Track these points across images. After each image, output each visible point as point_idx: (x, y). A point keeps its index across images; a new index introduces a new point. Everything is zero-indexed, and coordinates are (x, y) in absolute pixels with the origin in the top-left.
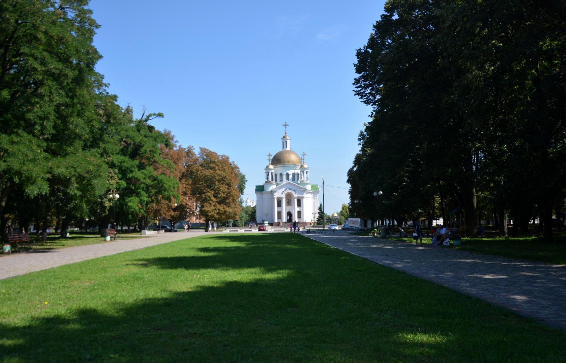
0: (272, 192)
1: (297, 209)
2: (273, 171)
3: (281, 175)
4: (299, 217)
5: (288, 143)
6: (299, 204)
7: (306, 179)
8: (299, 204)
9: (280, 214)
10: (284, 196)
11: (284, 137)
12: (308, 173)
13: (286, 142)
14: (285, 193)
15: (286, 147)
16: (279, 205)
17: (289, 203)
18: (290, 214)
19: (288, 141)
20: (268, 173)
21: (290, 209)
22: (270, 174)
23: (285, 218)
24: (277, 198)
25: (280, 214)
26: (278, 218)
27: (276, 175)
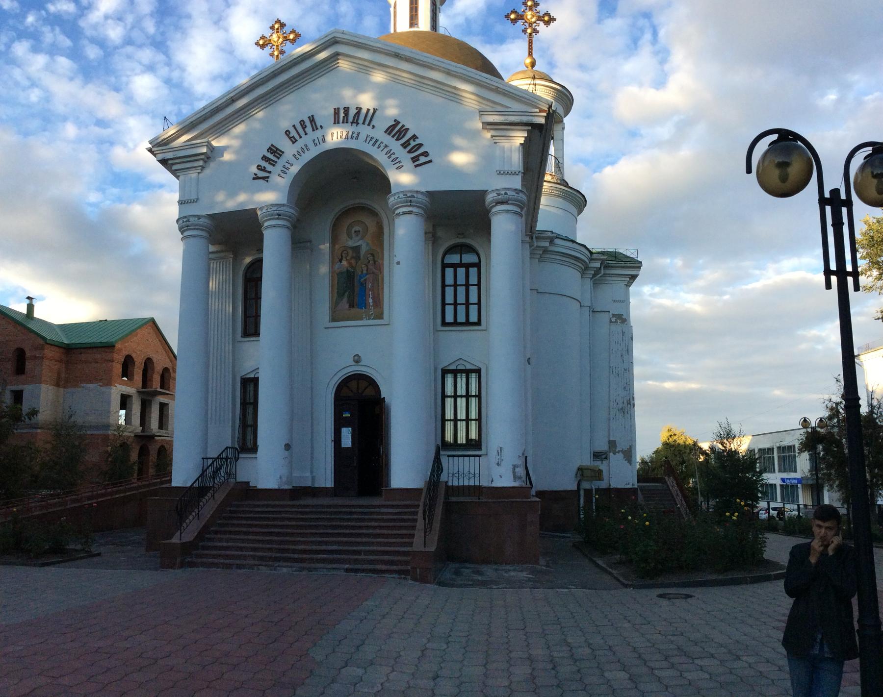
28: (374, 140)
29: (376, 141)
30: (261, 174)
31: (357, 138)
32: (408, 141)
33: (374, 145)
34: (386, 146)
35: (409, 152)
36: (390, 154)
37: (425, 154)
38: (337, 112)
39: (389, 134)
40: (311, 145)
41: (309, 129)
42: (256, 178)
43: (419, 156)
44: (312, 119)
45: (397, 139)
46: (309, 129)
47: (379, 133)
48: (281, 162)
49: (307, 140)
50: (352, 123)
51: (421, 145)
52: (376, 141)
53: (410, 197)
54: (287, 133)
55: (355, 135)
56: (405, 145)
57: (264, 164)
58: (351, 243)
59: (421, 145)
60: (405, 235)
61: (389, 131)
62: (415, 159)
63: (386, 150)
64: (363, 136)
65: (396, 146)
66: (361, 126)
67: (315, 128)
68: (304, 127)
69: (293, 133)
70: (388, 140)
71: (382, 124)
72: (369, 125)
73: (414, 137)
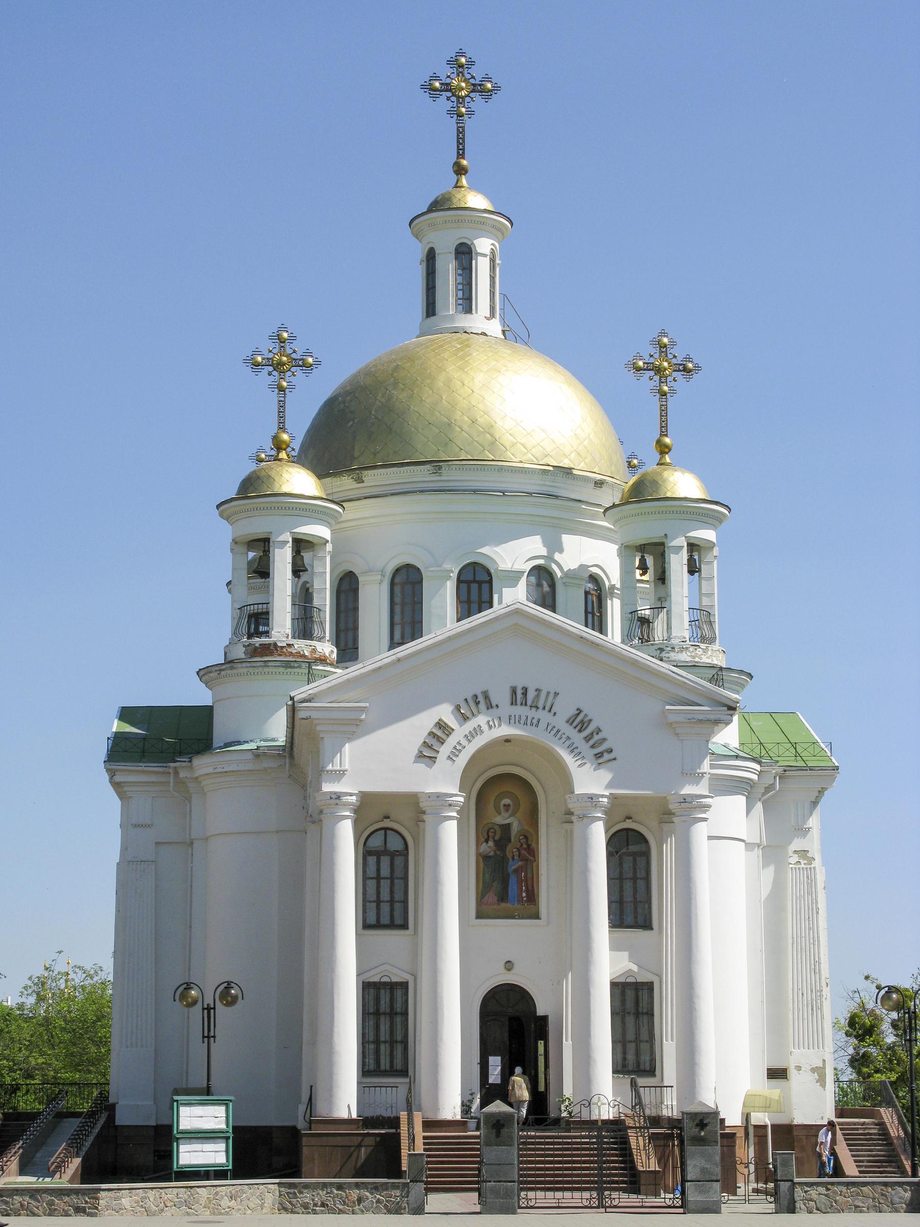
0: (296, 761)
1: (608, 960)
2: (322, 531)
3: (407, 585)
4: (636, 1056)
5: (482, 267)
6: (633, 907)
7: (682, 629)
8: (633, 907)
9: (389, 1013)
11: (439, 205)
12: (712, 568)
13: (465, 253)
15: (467, 304)
16: (390, 900)
17: (508, 877)
18: (514, 1029)
19: (483, 245)
20: (263, 544)
21: (519, 951)
22: (282, 560)
23: (449, 1076)
24: (367, 801)
26: (369, 1069)
27: (347, 587)
28: (555, 730)
29: (558, 731)
31: (537, 726)
32: (592, 734)
33: (555, 735)
34: (568, 738)
35: (593, 747)
37: (610, 751)
38: (514, 691)
39: (571, 724)
40: (485, 727)
41: (482, 706)
45: (580, 731)
47: (560, 722)
48: (451, 741)
50: (531, 707)
51: (604, 740)
52: (558, 731)
55: (535, 721)
56: (587, 739)
58: (500, 820)
59: (604, 740)
62: (599, 756)
63: (568, 743)
64: (543, 725)
65: (578, 738)
66: (540, 710)
67: (490, 706)
68: (477, 703)
71: (565, 709)
72: (550, 711)
73: (599, 730)
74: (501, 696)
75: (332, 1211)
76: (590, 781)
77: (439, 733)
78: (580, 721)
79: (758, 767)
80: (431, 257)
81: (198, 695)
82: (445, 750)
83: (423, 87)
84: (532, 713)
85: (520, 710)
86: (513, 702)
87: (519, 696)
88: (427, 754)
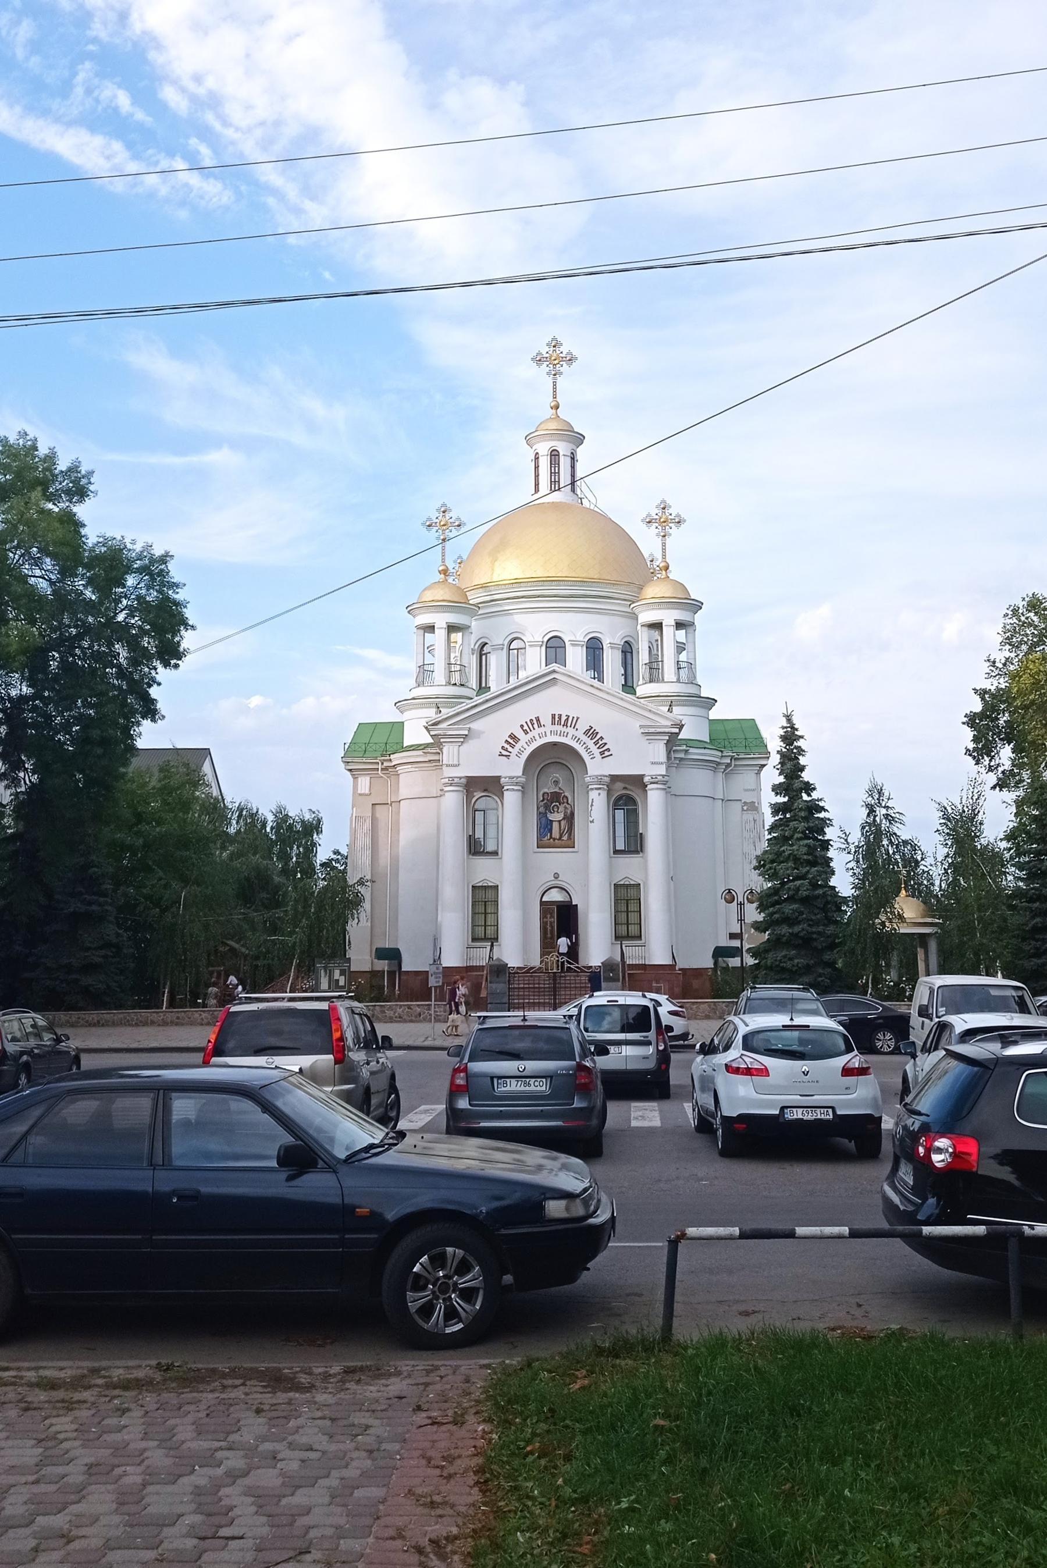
10: (512, 768)
14: (527, 746)
17: (554, 825)
25: (484, 901)
30: (504, 753)
36: (587, 749)
37: (608, 750)
38: (553, 716)
40: (537, 737)
41: (536, 726)
42: (501, 755)
43: (605, 752)
44: (538, 719)
46: (536, 726)
47: (580, 734)
48: (518, 746)
49: (534, 733)
53: (599, 779)
54: (522, 726)
56: (596, 743)
57: (506, 746)
60: (598, 801)
61: (586, 733)
62: (602, 753)
64: (570, 736)
65: (590, 743)
67: (540, 726)
69: (526, 727)
70: (584, 738)
71: (583, 726)
73: (602, 738)
74: (546, 720)
75: (405, 1021)
76: (597, 767)
77: (511, 741)
78: (591, 733)
79: (720, 754)
80: (537, 458)
81: (394, 717)
82: (514, 751)
83: (532, 359)
84: (564, 729)
85: (559, 728)
86: (553, 723)
87: (556, 719)
88: (504, 753)
